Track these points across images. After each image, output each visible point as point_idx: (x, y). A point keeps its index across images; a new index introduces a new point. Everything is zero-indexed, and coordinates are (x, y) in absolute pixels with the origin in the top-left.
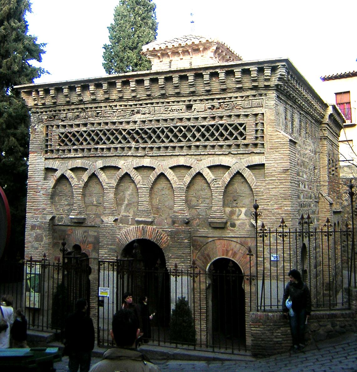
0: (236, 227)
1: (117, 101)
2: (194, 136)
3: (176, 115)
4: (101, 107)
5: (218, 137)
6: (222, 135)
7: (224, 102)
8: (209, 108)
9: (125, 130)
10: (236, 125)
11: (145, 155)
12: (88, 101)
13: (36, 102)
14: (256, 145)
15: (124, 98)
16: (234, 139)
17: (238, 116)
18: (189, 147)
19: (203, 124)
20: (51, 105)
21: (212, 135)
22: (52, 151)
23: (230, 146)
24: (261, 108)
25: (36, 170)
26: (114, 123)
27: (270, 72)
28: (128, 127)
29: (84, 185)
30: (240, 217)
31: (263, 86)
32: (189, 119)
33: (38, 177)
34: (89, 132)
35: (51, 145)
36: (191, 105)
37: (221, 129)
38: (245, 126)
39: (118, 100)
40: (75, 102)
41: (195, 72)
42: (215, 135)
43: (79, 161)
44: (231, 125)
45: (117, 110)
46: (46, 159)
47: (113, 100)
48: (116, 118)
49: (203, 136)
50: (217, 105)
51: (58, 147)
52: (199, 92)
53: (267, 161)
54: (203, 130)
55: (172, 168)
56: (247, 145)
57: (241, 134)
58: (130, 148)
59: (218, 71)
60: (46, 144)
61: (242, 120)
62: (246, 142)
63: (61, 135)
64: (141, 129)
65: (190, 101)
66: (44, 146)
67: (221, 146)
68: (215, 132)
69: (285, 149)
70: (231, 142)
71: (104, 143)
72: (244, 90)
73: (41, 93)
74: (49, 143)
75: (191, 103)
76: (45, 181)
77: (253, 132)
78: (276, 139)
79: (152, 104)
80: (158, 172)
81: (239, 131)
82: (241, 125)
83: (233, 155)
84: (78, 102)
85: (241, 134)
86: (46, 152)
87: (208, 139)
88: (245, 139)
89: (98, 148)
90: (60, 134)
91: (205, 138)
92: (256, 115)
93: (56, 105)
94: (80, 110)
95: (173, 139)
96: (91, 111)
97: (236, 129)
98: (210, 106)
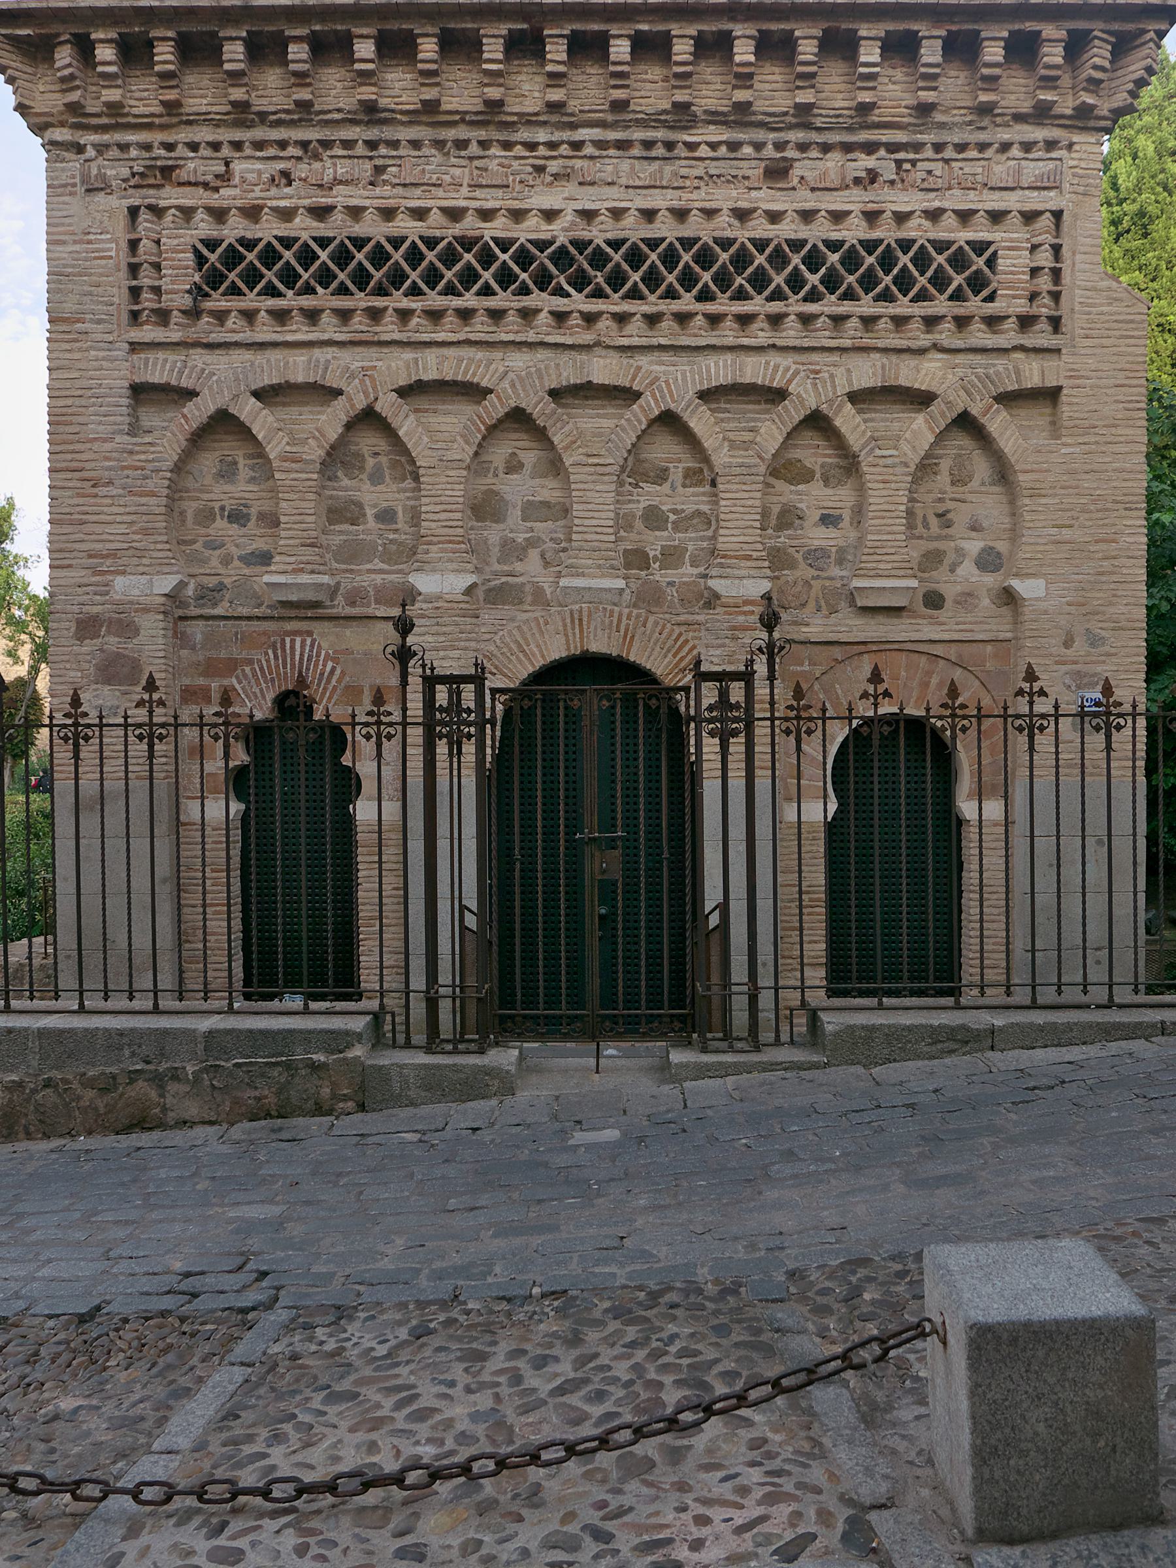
0: (949, 603)
1: (472, 123)
3: (725, 197)
4: (394, 144)
7: (914, 163)
8: (857, 181)
9: (504, 245)
11: (598, 344)
12: (339, 110)
13: (74, 96)
14: (1026, 322)
15: (508, 109)
16: (951, 298)
17: (965, 216)
18: (776, 320)
19: (835, 236)
20: (152, 115)
22: (163, 317)
23: (931, 322)
24: (1052, 194)
25: (89, 393)
26: (454, 214)
27: (1108, 55)
29: (328, 454)
30: (960, 571)
31: (1069, 112)
32: (774, 217)
33: (100, 423)
34: (342, 243)
35: (157, 290)
36: (782, 164)
37: (905, 260)
38: (995, 254)
39: (480, 118)
40: (275, 113)
41: (826, 25)
43: (300, 358)
45: (471, 158)
46: (135, 347)
47: (457, 117)
48: (465, 191)
50: (888, 170)
52: (823, 112)
54: (834, 258)
55: (705, 395)
56: (992, 322)
57: (977, 283)
58: (527, 314)
59: (922, 28)
60: (134, 283)
61: (980, 232)
62: (991, 308)
63: (205, 252)
64: (581, 245)
65: (780, 146)
66: (120, 296)
67: (900, 322)
69: (1132, 341)
70: (940, 305)
71: (415, 291)
72: (999, 120)
73: (105, 53)
74: (147, 282)
75: (790, 153)
76: (134, 440)
77: (1023, 273)
78: (1102, 305)
79: (623, 145)
80: (650, 405)
82: (980, 247)
83: (945, 356)
84: (287, 112)
85: (977, 283)
87: (849, 295)
88: (991, 298)
89: (386, 308)
90: (200, 246)
92: (1030, 217)
93: (175, 120)
94: (292, 151)
96: (350, 157)
97: (959, 261)
98: (863, 174)
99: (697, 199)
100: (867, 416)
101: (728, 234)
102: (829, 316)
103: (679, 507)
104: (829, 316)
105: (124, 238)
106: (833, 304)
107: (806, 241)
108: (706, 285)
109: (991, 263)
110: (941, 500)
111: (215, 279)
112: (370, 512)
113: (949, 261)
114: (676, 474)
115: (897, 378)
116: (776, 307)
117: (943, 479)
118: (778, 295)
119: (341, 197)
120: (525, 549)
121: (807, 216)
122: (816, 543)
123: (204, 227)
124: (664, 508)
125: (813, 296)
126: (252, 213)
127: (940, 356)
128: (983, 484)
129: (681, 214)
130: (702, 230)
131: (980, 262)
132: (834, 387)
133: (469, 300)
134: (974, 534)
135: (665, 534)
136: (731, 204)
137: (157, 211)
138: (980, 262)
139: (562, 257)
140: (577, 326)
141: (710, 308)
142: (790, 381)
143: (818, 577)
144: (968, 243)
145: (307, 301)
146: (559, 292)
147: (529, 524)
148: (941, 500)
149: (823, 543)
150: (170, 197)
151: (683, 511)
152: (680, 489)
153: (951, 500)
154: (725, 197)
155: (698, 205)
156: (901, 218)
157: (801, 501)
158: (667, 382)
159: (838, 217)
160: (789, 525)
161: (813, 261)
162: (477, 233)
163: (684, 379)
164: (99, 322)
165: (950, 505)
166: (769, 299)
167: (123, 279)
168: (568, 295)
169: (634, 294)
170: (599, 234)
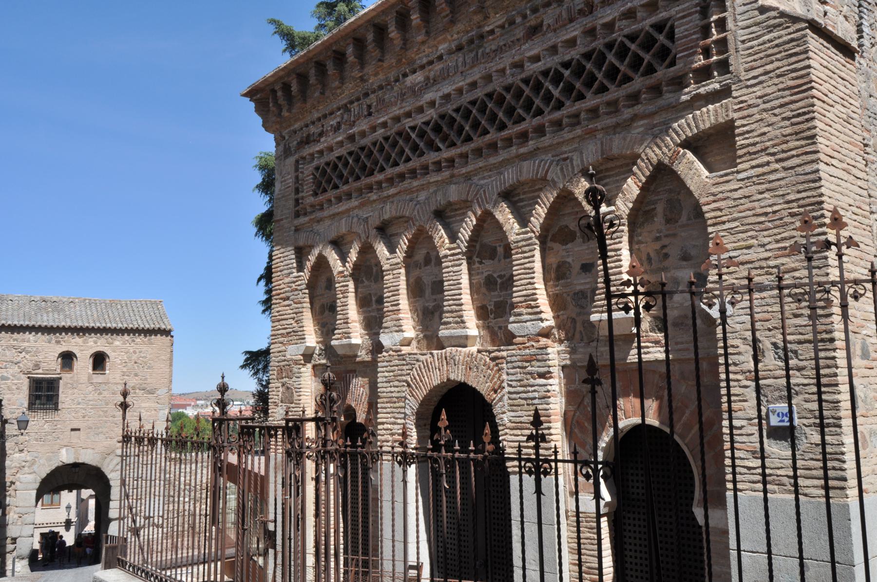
2: (548, 97)
5: (605, 82)
6: (613, 74)
10: (647, 32)
16: (643, 75)
19: (567, 58)
21: (591, 81)
26: (397, 119)
28: (419, 120)
32: (536, 59)
35: (303, 198)
37: (611, 57)
42: (597, 79)
44: (632, 38)
49: (569, 89)
51: (312, 199)
53: (740, 109)
54: (567, 73)
66: (291, 203)
68: (596, 72)
77: (694, 33)
81: (657, 45)
82: (659, 27)
83: (645, 121)
86: (297, 215)
87: (581, 97)
88: (673, 63)
91: (574, 94)
95: (505, 120)
97: (649, 43)
99: (494, 66)
100: (605, 181)
101: (510, 80)
102: (569, 117)
103: (503, 273)
104: (569, 117)
105: (293, 175)
106: (572, 106)
107: (550, 69)
108: (501, 120)
109: (671, 36)
110: (658, 239)
111: (319, 184)
112: (374, 299)
113: (639, 45)
114: (500, 250)
115: (611, 149)
116: (537, 120)
117: (659, 219)
118: (540, 112)
119: (355, 130)
120: (432, 313)
121: (553, 49)
122: (578, 288)
123: (315, 163)
124: (495, 275)
125: (560, 105)
126: (331, 149)
127: (642, 122)
128: (689, 219)
129: (488, 78)
130: (496, 85)
131: (661, 38)
132: (573, 168)
133: (402, 168)
134: (685, 263)
135: (496, 293)
136: (510, 60)
137: (304, 158)
138: (661, 38)
139: (437, 129)
140: (445, 167)
141: (505, 133)
142: (547, 172)
143: (579, 314)
144: (652, 26)
145: (345, 188)
146: (438, 149)
147: (434, 297)
148: (658, 239)
149: (582, 287)
150: (307, 151)
151: (504, 276)
152: (503, 260)
153: (666, 236)
154: (506, 60)
155: (494, 69)
156: (609, 27)
157: (568, 256)
158: (484, 191)
159: (571, 43)
160: (562, 278)
161: (557, 78)
162: (402, 128)
163: (492, 188)
164: (287, 218)
165: (666, 241)
166: (534, 116)
167: (293, 196)
168: (438, 149)
169: (469, 139)
170: (449, 108)
